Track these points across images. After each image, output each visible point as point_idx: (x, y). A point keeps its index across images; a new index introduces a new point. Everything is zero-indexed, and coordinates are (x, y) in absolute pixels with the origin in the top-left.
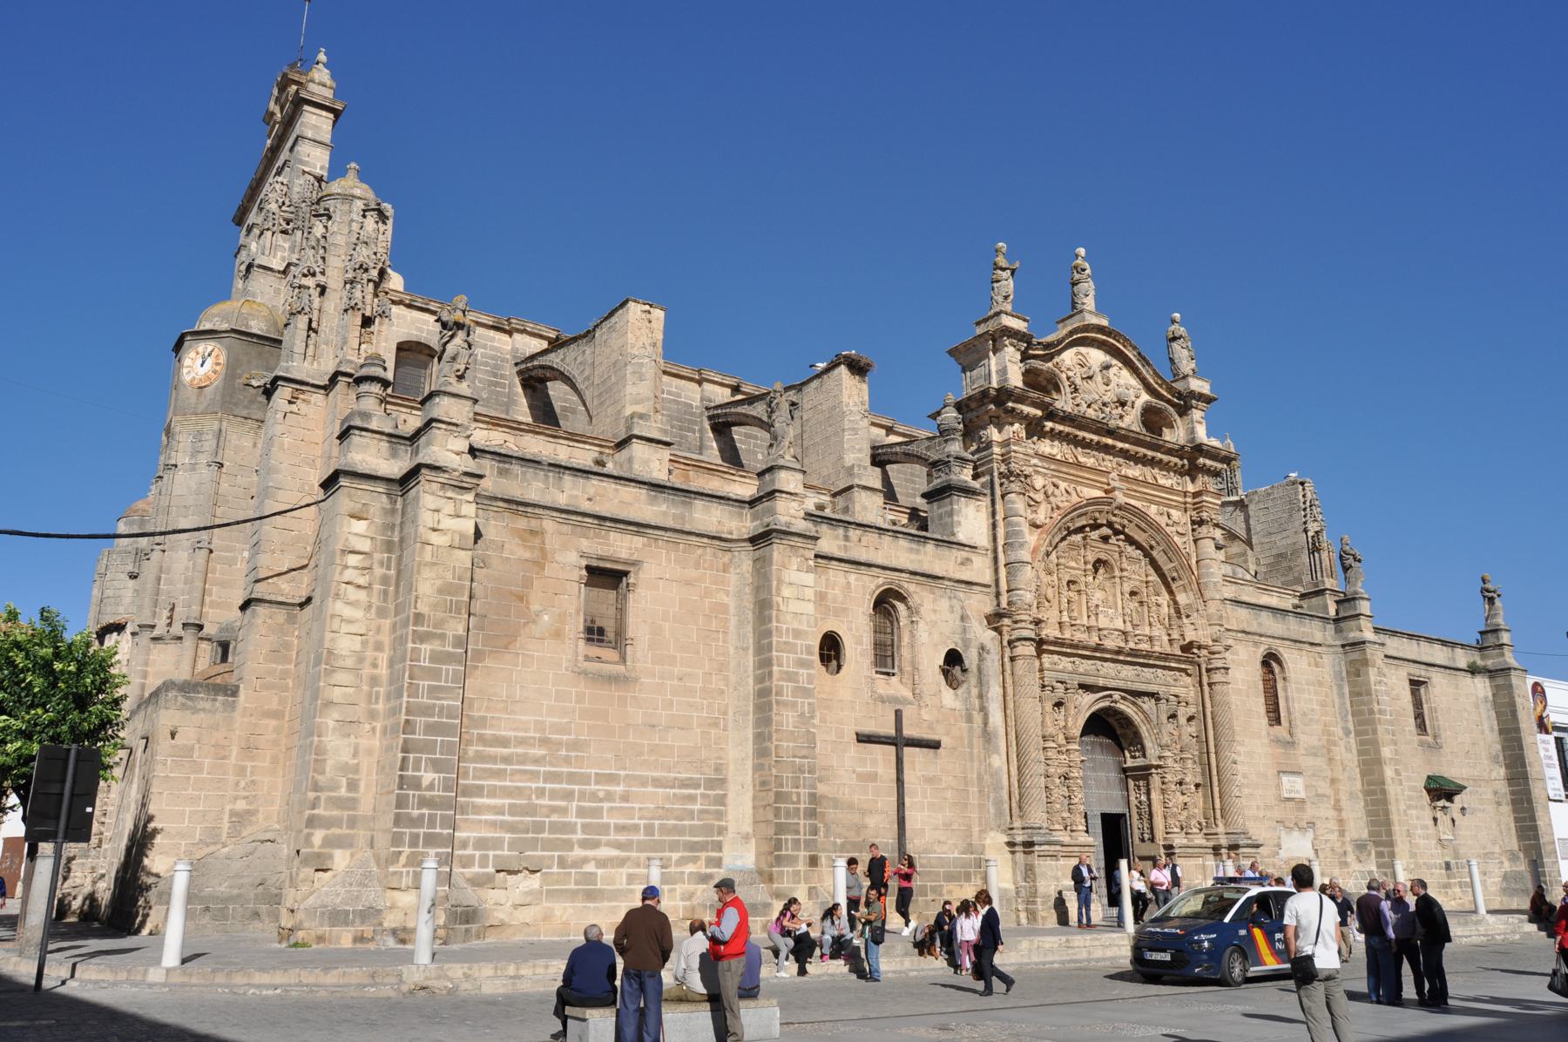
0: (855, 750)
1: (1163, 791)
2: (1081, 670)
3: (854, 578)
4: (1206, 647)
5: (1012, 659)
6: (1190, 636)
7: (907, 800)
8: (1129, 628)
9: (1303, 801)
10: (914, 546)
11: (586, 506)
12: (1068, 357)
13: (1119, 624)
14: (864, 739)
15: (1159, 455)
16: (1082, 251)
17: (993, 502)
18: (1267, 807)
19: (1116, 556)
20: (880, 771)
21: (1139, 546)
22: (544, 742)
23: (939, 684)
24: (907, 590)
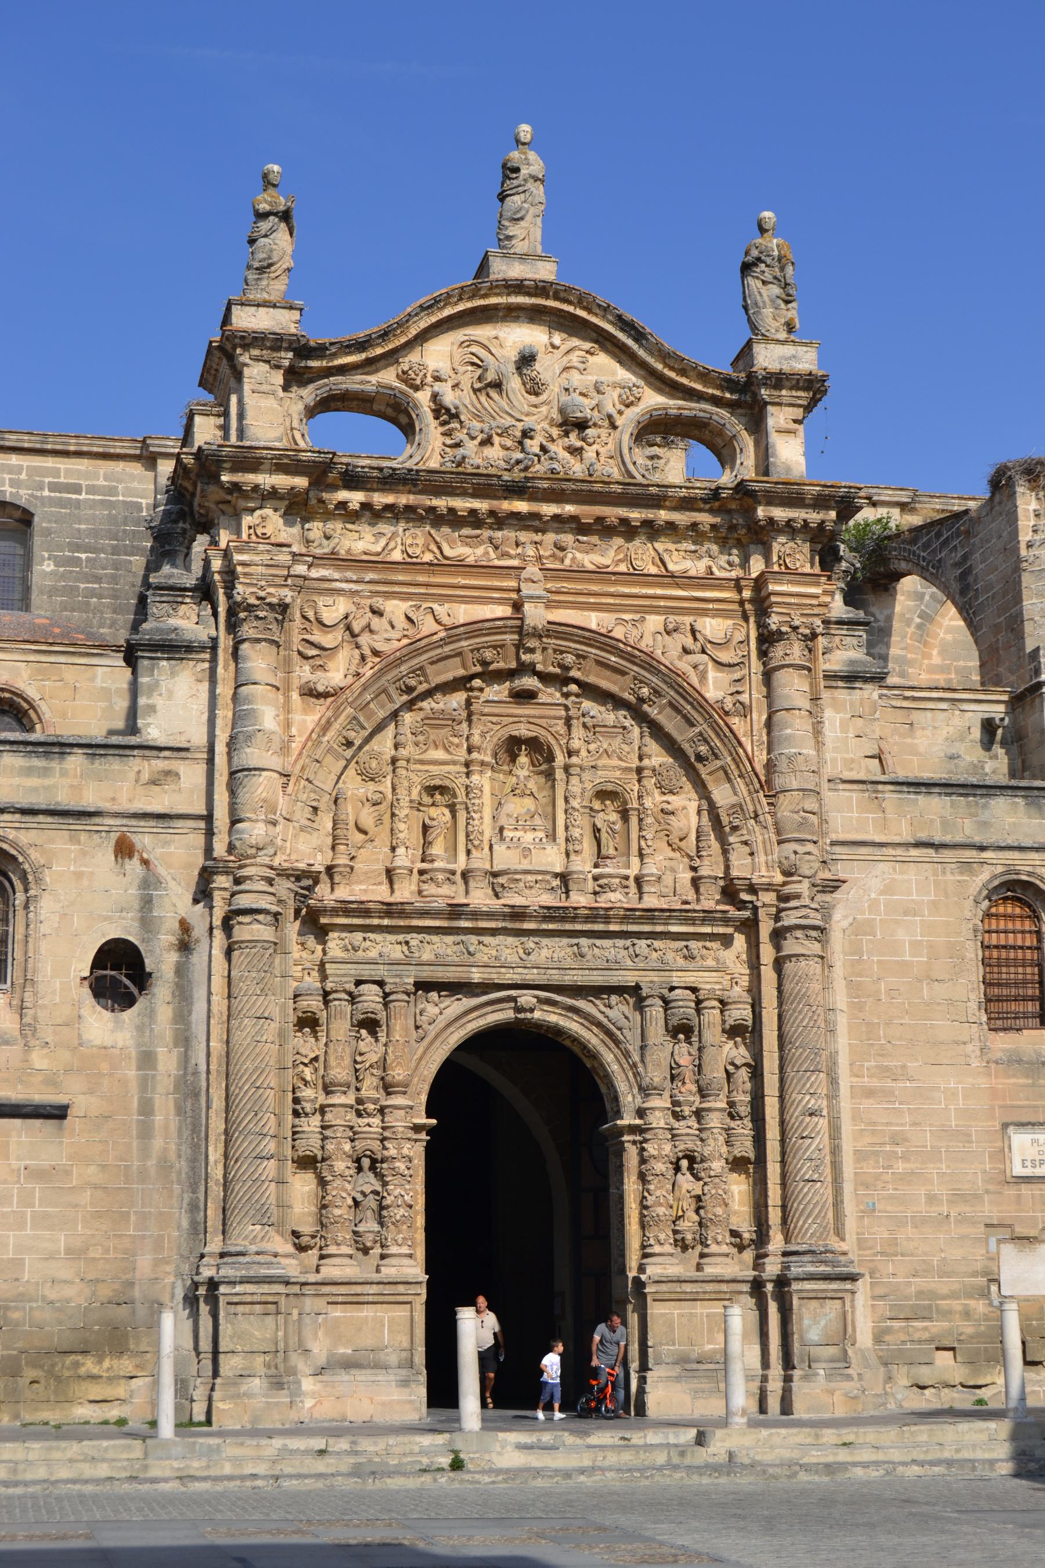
1: (642, 1177)
2: (427, 956)
4: (769, 887)
5: (229, 952)
8: (583, 864)
10: (37, 762)
12: (439, 355)
13: (552, 859)
15: (663, 515)
16: (525, 131)
17: (214, 660)
18: (958, 1197)
19: (560, 727)
23: (78, 1004)
24: (14, 844)
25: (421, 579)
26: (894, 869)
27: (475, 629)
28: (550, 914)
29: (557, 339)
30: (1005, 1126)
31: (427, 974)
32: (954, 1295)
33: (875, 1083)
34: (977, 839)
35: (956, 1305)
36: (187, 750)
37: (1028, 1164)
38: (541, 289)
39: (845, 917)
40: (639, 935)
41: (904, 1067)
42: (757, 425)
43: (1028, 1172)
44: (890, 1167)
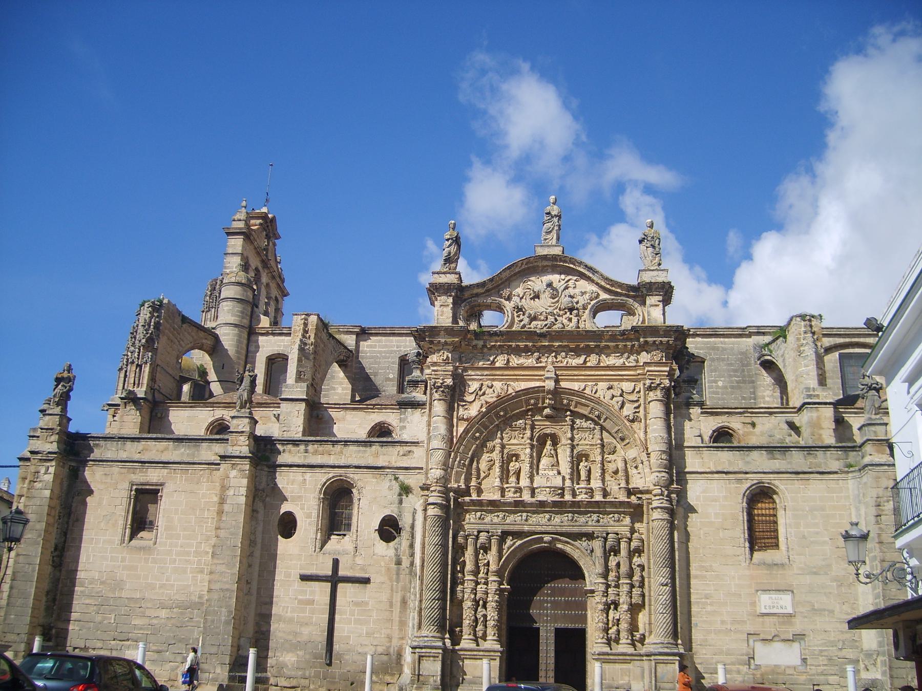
0: (298, 585)
3: (309, 475)
6: (637, 482)
7: (337, 617)
9: (790, 615)
10: (361, 448)
11: (137, 457)
13: (558, 482)
14: (305, 578)
20: (317, 598)
21: (587, 419)
22: (102, 583)
24: (352, 479)
25: (506, 373)
27: (527, 391)
28: (555, 504)
29: (563, 277)
30: (757, 591)
31: (506, 528)
32: (733, 664)
34: (745, 469)
35: (734, 668)
36: (418, 443)
38: (554, 258)
40: (594, 513)
42: (643, 303)
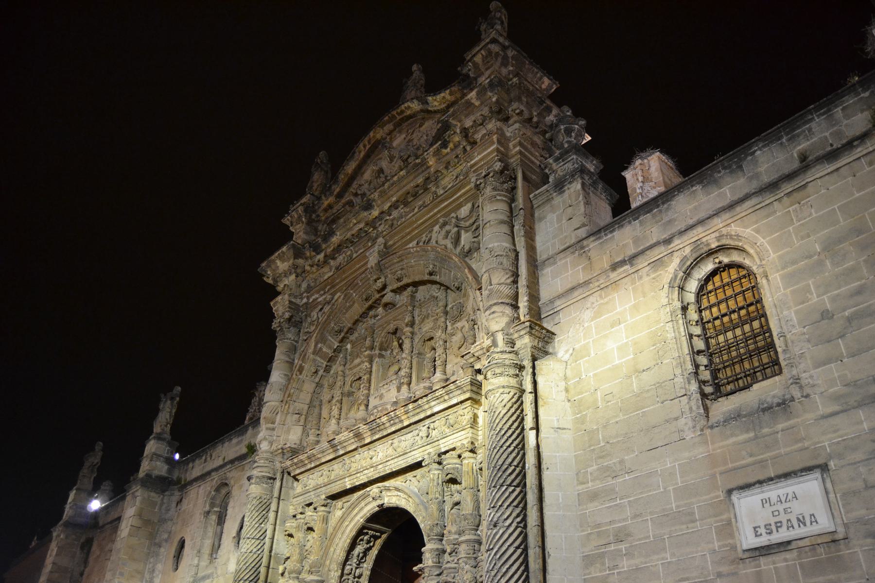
9: (833, 541)
26: (601, 296)
30: (730, 492)
33: (598, 485)
37: (762, 530)
39: (567, 351)
41: (622, 462)
43: (764, 540)
44: (616, 567)
